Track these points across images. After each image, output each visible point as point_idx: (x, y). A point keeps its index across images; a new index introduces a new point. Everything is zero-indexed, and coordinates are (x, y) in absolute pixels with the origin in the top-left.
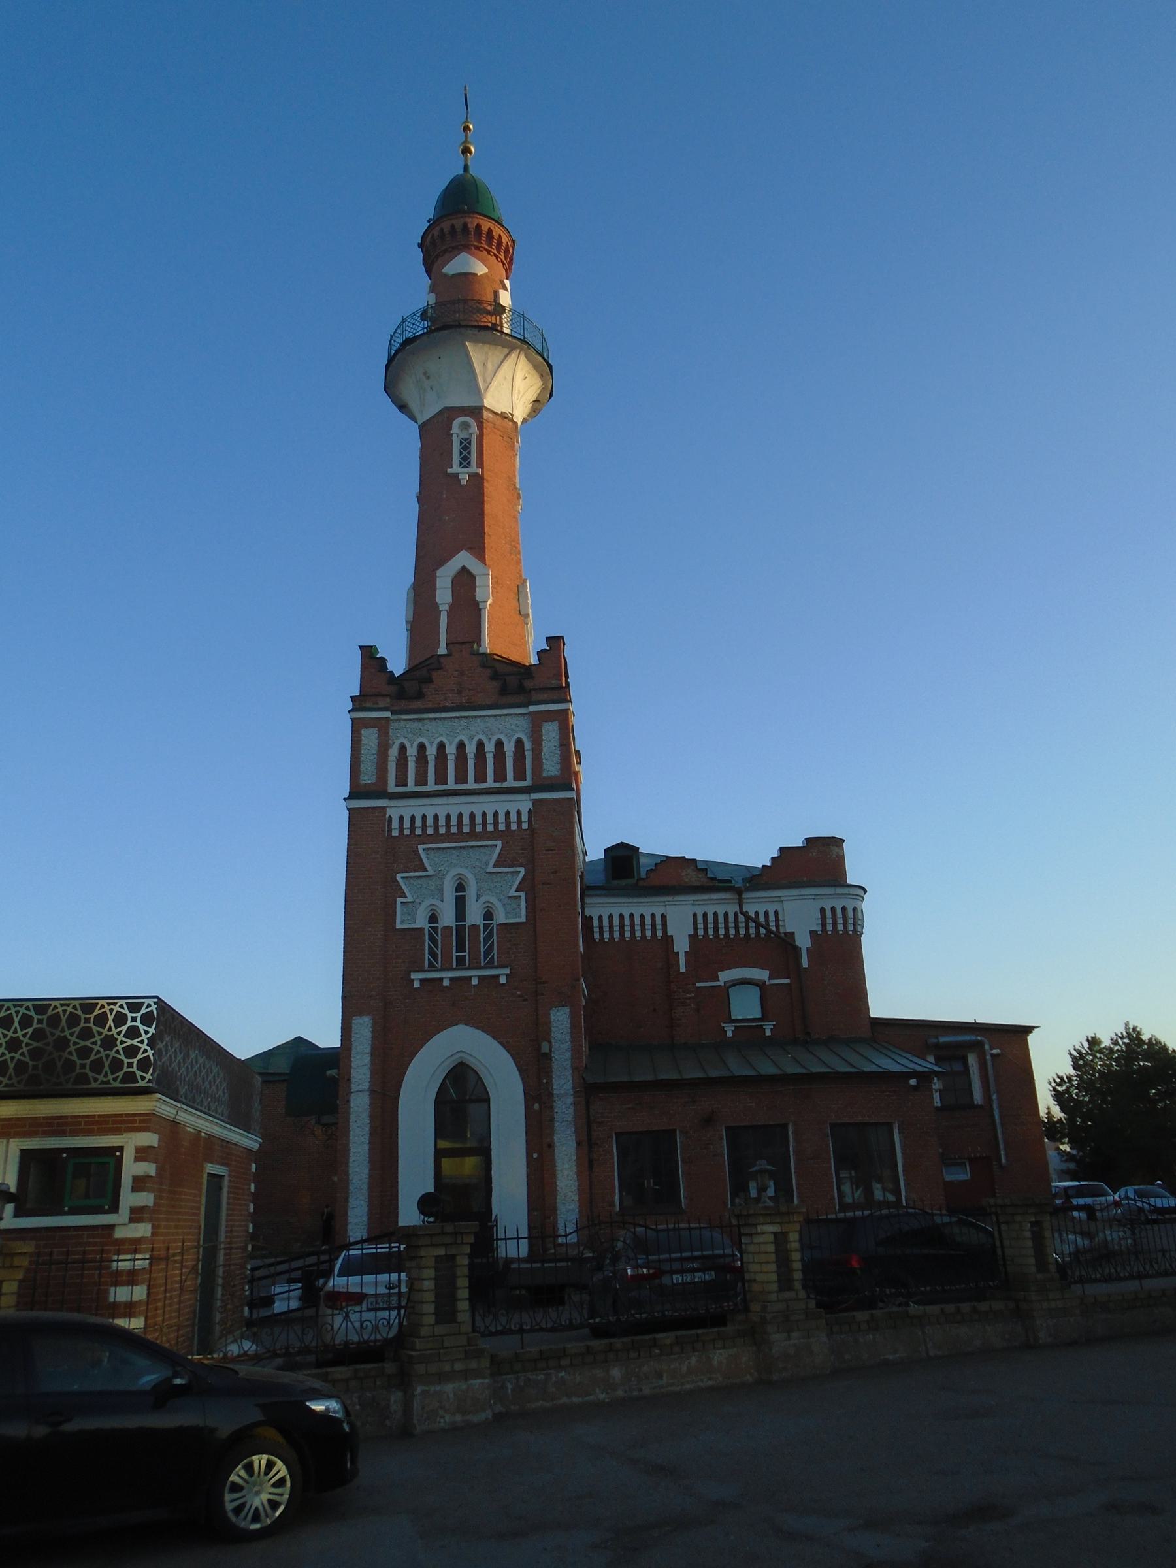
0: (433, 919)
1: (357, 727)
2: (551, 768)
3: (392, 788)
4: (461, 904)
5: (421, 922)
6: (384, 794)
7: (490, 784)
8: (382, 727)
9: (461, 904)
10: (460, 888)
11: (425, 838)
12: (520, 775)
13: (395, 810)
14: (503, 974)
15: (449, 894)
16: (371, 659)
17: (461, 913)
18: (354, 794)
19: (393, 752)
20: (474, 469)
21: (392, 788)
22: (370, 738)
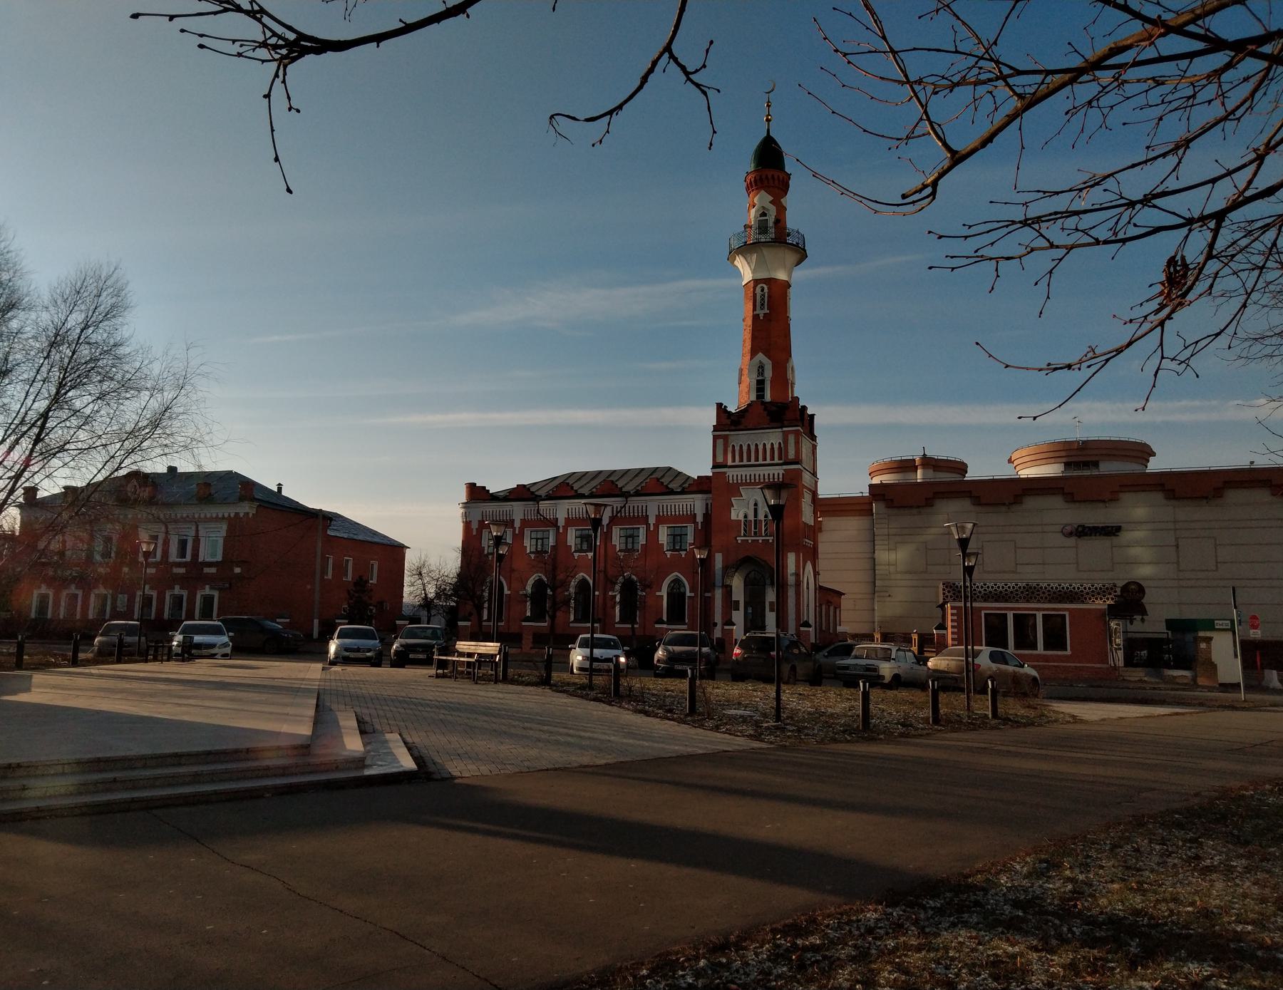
0: (746, 516)
1: (715, 438)
2: (791, 455)
3: (730, 463)
4: (756, 510)
5: (741, 517)
6: (726, 466)
7: (768, 461)
8: (726, 438)
9: (756, 510)
10: (756, 504)
11: (742, 484)
12: (780, 458)
13: (731, 473)
14: (770, 539)
15: (752, 507)
16: (721, 408)
17: (756, 515)
18: (714, 467)
19: (730, 449)
20: (767, 311)
21: (730, 463)
22: (720, 442)
